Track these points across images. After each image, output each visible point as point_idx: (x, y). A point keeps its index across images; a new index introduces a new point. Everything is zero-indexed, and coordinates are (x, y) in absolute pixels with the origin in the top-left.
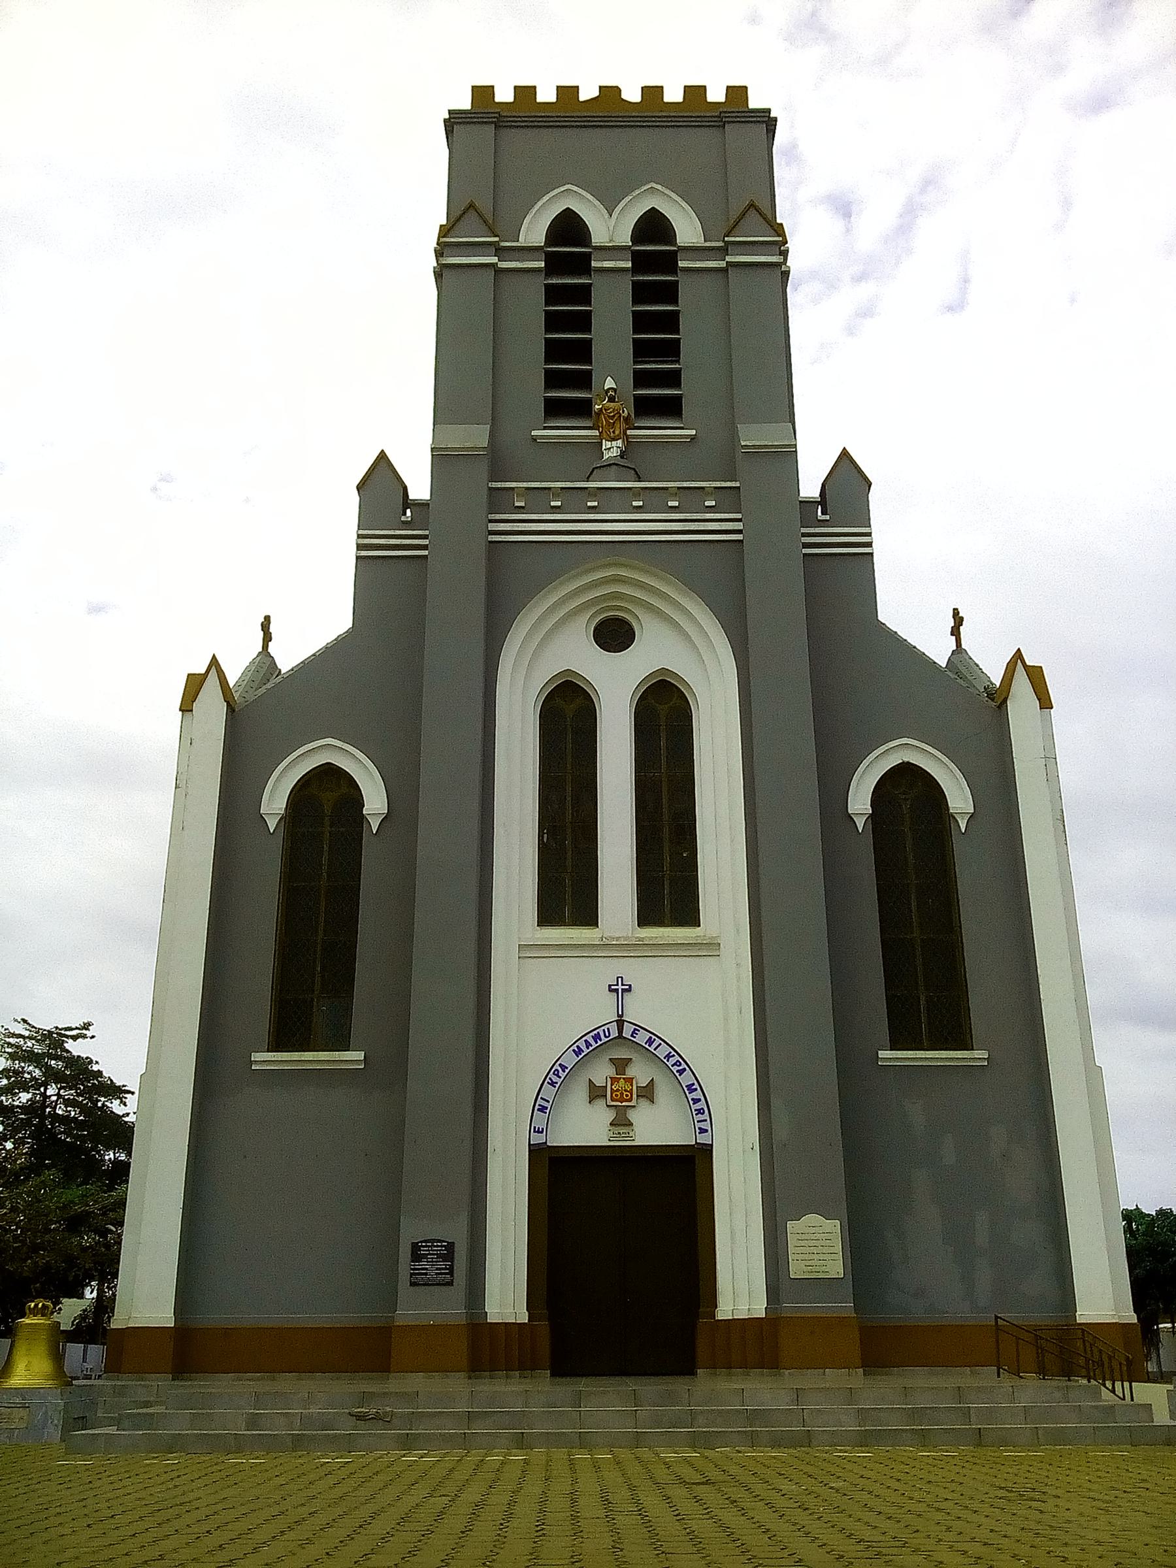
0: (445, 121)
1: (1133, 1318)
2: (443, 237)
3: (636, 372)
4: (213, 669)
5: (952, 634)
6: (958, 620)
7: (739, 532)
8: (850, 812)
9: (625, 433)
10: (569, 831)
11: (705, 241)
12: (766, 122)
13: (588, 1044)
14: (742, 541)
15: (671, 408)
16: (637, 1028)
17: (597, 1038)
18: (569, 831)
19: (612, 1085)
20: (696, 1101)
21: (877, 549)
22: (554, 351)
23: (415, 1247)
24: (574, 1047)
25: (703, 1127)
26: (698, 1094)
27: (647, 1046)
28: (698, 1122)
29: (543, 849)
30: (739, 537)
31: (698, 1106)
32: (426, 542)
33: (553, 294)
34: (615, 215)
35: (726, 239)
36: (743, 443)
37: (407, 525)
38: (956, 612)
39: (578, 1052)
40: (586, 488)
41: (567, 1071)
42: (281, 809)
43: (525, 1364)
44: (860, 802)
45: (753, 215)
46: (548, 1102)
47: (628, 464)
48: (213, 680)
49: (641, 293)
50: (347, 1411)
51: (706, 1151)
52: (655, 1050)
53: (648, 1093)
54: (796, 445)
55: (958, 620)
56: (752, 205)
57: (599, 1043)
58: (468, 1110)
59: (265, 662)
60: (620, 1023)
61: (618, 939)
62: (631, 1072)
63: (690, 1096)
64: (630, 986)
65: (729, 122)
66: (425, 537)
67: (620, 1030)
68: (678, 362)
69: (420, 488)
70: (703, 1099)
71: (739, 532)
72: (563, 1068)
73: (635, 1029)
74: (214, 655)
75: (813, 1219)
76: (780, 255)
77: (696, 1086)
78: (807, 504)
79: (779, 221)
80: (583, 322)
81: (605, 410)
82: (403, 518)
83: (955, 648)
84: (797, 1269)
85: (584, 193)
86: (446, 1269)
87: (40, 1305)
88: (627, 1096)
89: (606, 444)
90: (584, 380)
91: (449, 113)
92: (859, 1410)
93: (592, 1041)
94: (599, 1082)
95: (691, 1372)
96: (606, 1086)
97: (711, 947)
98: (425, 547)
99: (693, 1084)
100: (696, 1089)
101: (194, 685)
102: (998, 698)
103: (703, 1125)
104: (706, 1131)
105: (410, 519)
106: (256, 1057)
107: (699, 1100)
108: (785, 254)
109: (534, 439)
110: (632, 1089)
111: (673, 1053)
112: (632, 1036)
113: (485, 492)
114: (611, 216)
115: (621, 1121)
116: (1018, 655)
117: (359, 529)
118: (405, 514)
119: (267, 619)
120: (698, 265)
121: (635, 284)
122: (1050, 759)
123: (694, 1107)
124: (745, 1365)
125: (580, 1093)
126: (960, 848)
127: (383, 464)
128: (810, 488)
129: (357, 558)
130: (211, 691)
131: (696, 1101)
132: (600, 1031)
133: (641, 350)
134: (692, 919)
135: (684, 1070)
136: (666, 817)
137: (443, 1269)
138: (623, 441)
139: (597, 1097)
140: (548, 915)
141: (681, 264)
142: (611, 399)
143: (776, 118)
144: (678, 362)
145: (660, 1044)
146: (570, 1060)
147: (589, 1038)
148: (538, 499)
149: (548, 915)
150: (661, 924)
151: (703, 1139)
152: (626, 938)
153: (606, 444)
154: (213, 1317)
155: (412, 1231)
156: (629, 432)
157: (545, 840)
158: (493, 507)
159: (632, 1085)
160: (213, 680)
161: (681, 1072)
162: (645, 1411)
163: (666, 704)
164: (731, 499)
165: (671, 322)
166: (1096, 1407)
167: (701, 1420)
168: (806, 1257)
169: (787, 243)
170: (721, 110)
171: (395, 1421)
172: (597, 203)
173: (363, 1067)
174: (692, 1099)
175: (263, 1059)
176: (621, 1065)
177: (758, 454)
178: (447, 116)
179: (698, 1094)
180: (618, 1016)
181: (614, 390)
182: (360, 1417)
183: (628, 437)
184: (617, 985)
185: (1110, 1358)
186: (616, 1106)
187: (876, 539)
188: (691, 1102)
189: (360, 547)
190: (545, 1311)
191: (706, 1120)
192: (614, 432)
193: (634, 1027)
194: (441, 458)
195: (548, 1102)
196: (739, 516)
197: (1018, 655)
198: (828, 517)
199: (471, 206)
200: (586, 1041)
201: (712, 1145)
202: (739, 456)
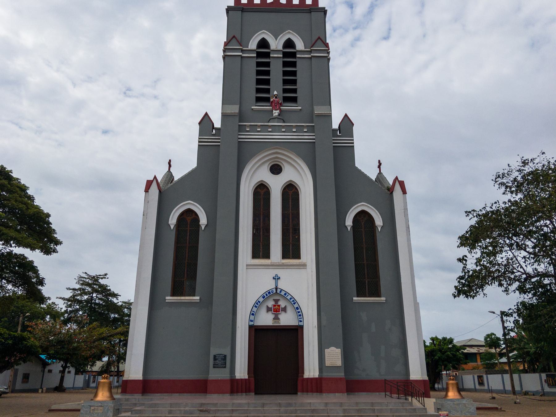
0: (226, 9)
1: (426, 378)
2: (226, 46)
3: (283, 80)
4: (155, 180)
5: (378, 168)
6: (380, 164)
7: (314, 139)
8: (346, 225)
9: (280, 108)
10: (262, 230)
11: (305, 49)
12: (324, 11)
13: (267, 295)
14: (314, 142)
15: (294, 100)
16: (281, 290)
17: (269, 293)
18: (262, 230)
19: (274, 307)
20: (299, 312)
21: (355, 145)
22: (259, 82)
23: (215, 356)
24: (263, 296)
25: (301, 320)
26: (299, 310)
27: (284, 296)
28: (299, 318)
29: (254, 235)
30: (314, 141)
31: (299, 314)
32: (219, 140)
33: (259, 64)
34: (278, 40)
35: (311, 48)
36: (315, 113)
37: (214, 135)
38: (379, 161)
39: (264, 297)
40: (268, 125)
41: (260, 303)
42: (175, 222)
43: (247, 390)
44: (349, 222)
45: (319, 41)
46: (255, 312)
47: (280, 118)
48: (155, 182)
49: (285, 64)
50: (197, 409)
51: (302, 327)
52: (287, 297)
53: (285, 310)
54: (331, 114)
55: (380, 164)
56: (319, 38)
57: (270, 294)
58: (231, 316)
59: (169, 176)
60: (276, 288)
61: (276, 263)
62: (279, 303)
63: (297, 311)
64: (279, 277)
65: (313, 11)
66: (219, 139)
67: (276, 290)
68: (296, 85)
69: (218, 124)
70: (301, 312)
71: (314, 139)
72: (259, 302)
73: (281, 290)
74: (155, 175)
75: (333, 348)
76: (327, 54)
77: (299, 308)
78: (334, 131)
79: (327, 42)
80: (268, 73)
81: (274, 101)
82: (212, 133)
83: (379, 172)
84: (328, 363)
85: (268, 33)
86: (224, 363)
87: (106, 376)
88: (278, 310)
89: (274, 111)
90: (268, 91)
91: (228, 7)
92: (343, 409)
93: (268, 294)
94: (270, 306)
95: (295, 393)
96: (272, 308)
97: (304, 266)
98: (219, 142)
99: (298, 307)
100: (299, 309)
101: (149, 184)
102: (391, 190)
103: (301, 320)
104: (302, 321)
105: (214, 133)
106: (167, 298)
107: (300, 312)
108: (329, 53)
109: (252, 109)
110: (279, 309)
111: (292, 298)
112: (280, 292)
113: (237, 127)
114: (276, 40)
115: (276, 318)
116: (397, 178)
117: (199, 136)
118: (213, 132)
119: (170, 161)
120: (303, 56)
121: (284, 62)
122: (406, 209)
123: (298, 314)
124: (312, 391)
125: (263, 310)
126: (379, 237)
127: (206, 116)
128: (335, 125)
129: (199, 145)
130: (154, 186)
131: (299, 312)
132: (270, 291)
133: (285, 82)
134: (299, 257)
135: (295, 303)
136: (291, 226)
137: (222, 363)
138: (279, 111)
139: (269, 310)
140: (255, 256)
141: (298, 56)
142: (276, 98)
143: (327, 10)
144: (296, 85)
145: (288, 295)
146: (261, 300)
147: (267, 293)
148: (253, 128)
149: (255, 256)
150: (288, 258)
151: (301, 324)
152: (278, 263)
153: (274, 111)
154: (154, 376)
155: (214, 351)
156: (281, 108)
157: (254, 232)
158: (239, 132)
159: (280, 307)
160: (154, 183)
161: (294, 303)
162: (283, 409)
163: (291, 191)
164: (312, 129)
165: (294, 73)
166: (411, 409)
167: (298, 412)
168: (331, 360)
169: (329, 49)
170: (310, 7)
171: (211, 412)
172: (272, 36)
173: (199, 301)
174: (298, 312)
175: (169, 298)
176: (276, 301)
177: (320, 116)
178: (227, 8)
179: (299, 310)
180: (276, 286)
181: (277, 95)
182: (201, 411)
183: (280, 109)
184: (276, 277)
185: (418, 391)
186: (274, 314)
187: (355, 141)
188: (297, 313)
189: (199, 142)
190: (253, 375)
191: (301, 318)
192: (277, 108)
193: (280, 290)
194: (225, 116)
195: (255, 312)
196: (314, 134)
197: (397, 178)
198: (341, 134)
199: (234, 37)
200: (266, 294)
201: (303, 326)
202: (314, 117)
